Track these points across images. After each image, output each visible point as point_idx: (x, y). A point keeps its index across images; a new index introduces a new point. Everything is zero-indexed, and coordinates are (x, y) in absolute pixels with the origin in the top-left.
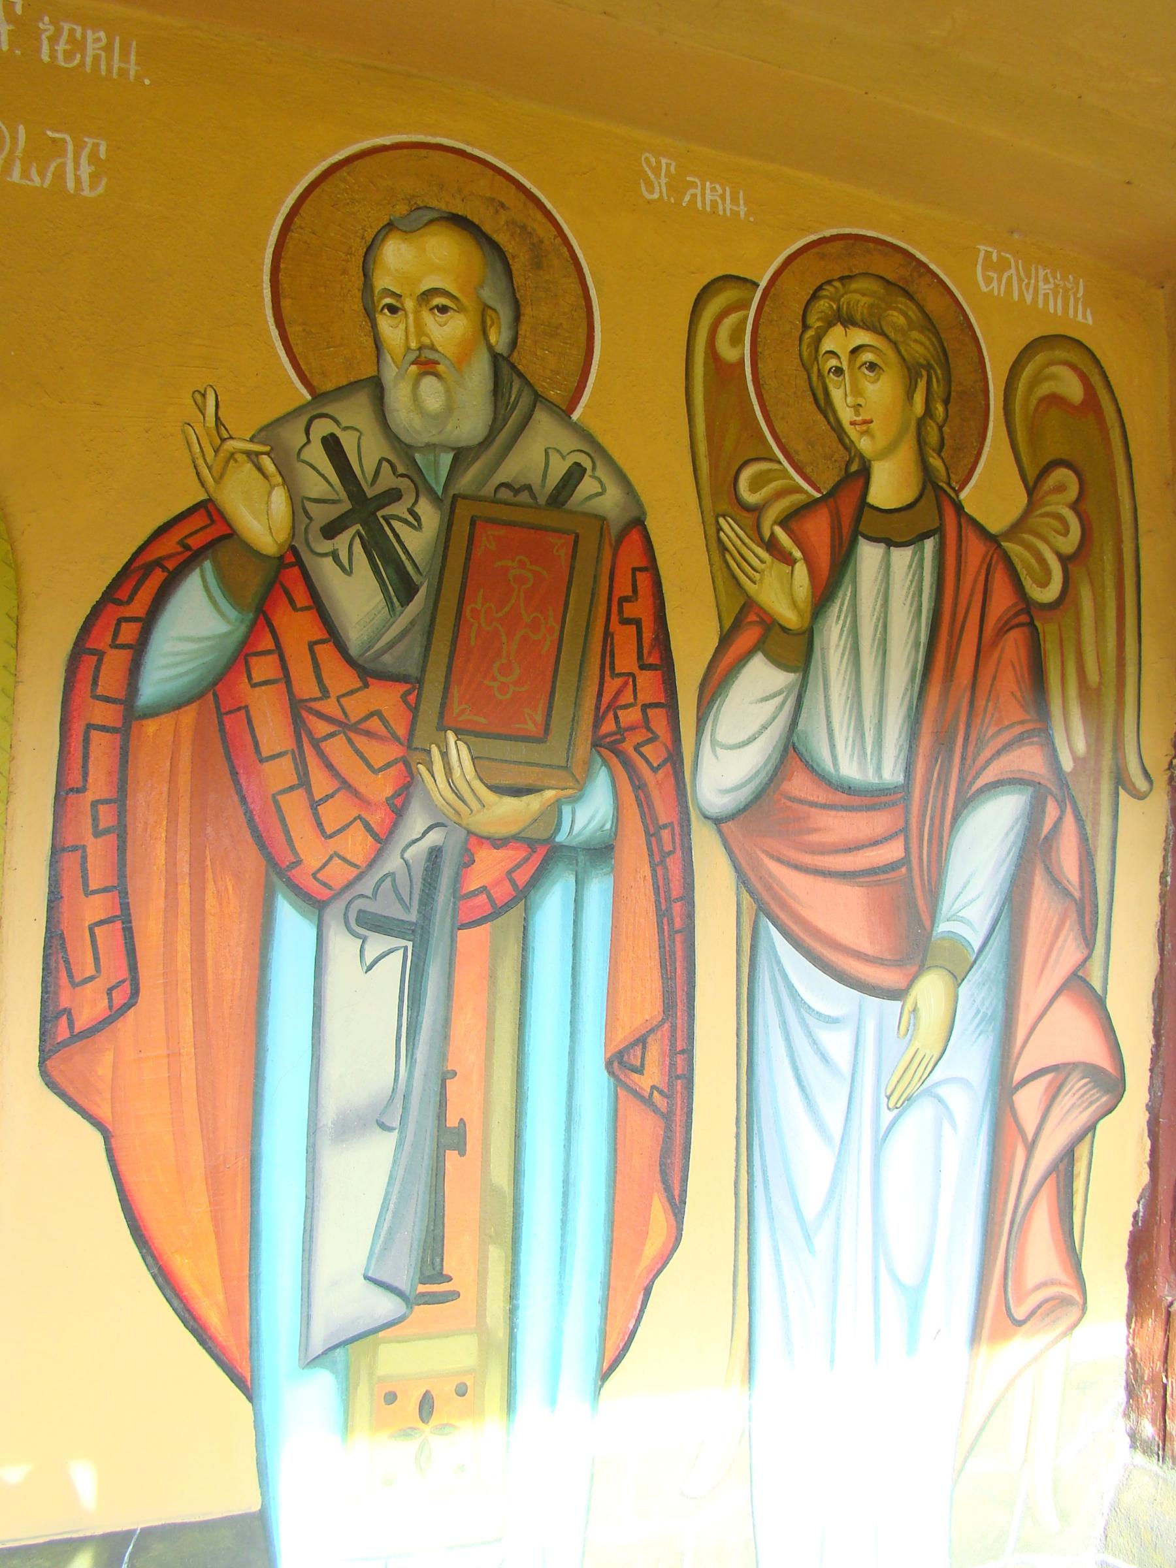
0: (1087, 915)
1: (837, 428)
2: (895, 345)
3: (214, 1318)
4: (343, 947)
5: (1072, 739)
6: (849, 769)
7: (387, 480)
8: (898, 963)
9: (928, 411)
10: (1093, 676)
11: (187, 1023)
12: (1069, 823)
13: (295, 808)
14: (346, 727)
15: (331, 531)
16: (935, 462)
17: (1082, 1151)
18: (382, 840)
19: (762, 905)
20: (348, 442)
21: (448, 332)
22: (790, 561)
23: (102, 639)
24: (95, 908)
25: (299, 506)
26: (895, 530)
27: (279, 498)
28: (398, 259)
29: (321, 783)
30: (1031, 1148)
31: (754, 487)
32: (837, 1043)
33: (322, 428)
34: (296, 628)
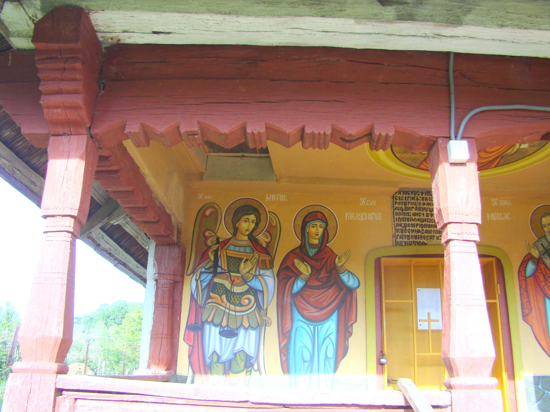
11: (538, 313)
15: (544, 254)
20: (543, 243)
25: (539, 252)
27: (537, 252)
28: (544, 220)
33: (540, 242)
34: (542, 266)
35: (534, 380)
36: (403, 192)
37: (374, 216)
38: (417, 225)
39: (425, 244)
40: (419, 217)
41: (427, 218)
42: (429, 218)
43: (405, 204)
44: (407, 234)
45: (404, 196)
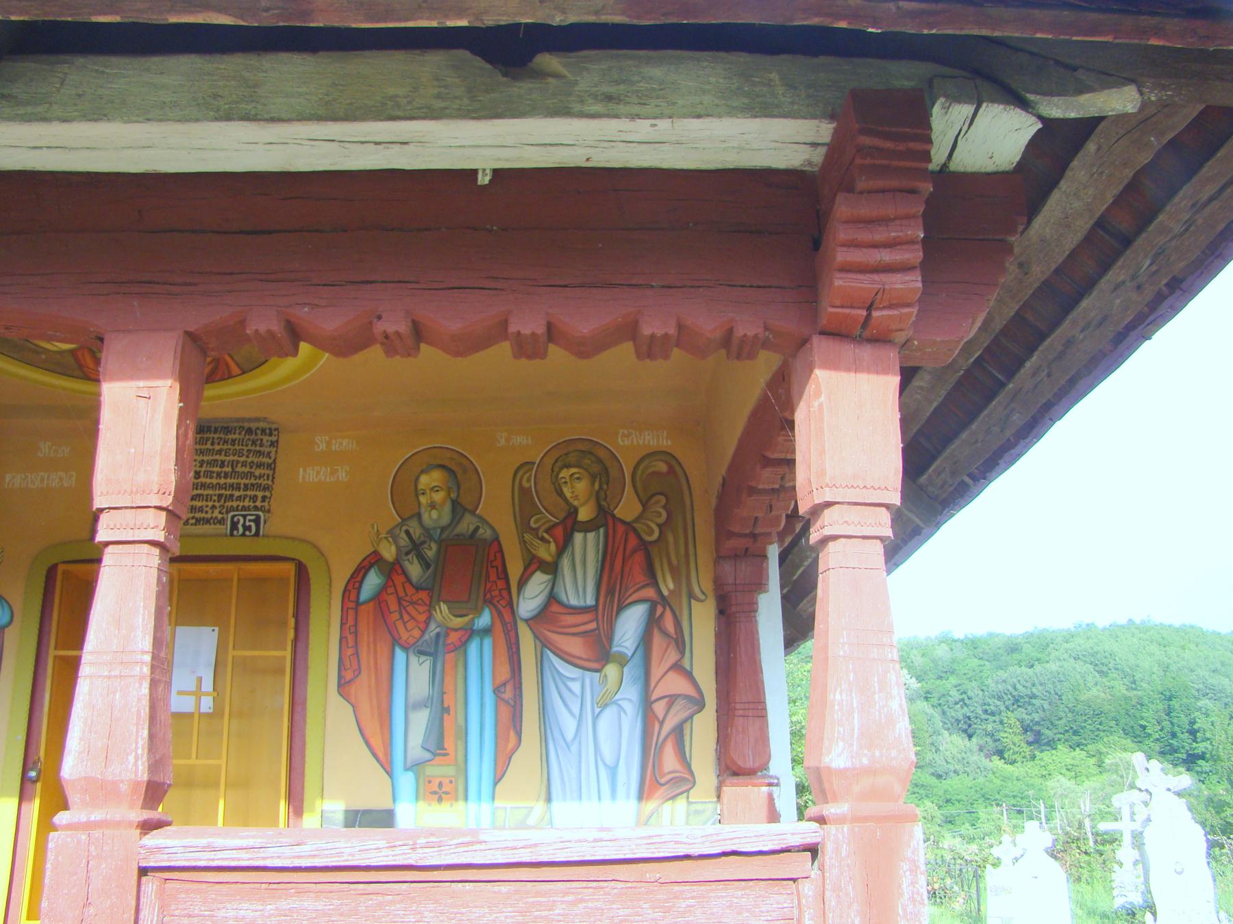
0: (680, 642)
1: (565, 499)
2: (586, 470)
3: (381, 755)
4: (414, 659)
5: (668, 585)
6: (573, 601)
7: (422, 539)
8: (597, 661)
9: (601, 487)
10: (674, 561)
11: (373, 680)
12: (668, 613)
13: (400, 625)
14: (412, 603)
15: (407, 554)
16: (603, 503)
17: (687, 726)
18: (423, 632)
19: (544, 644)
20: (411, 531)
21: (438, 497)
22: (549, 542)
23: (350, 587)
24: (350, 652)
25: (398, 549)
26: (587, 527)
27: (393, 548)
28: (424, 479)
29: (406, 617)
30: (662, 723)
31: (536, 522)
32: (576, 687)
33: (404, 528)
34: (399, 580)
35: (346, 818)
37: (61, 479)
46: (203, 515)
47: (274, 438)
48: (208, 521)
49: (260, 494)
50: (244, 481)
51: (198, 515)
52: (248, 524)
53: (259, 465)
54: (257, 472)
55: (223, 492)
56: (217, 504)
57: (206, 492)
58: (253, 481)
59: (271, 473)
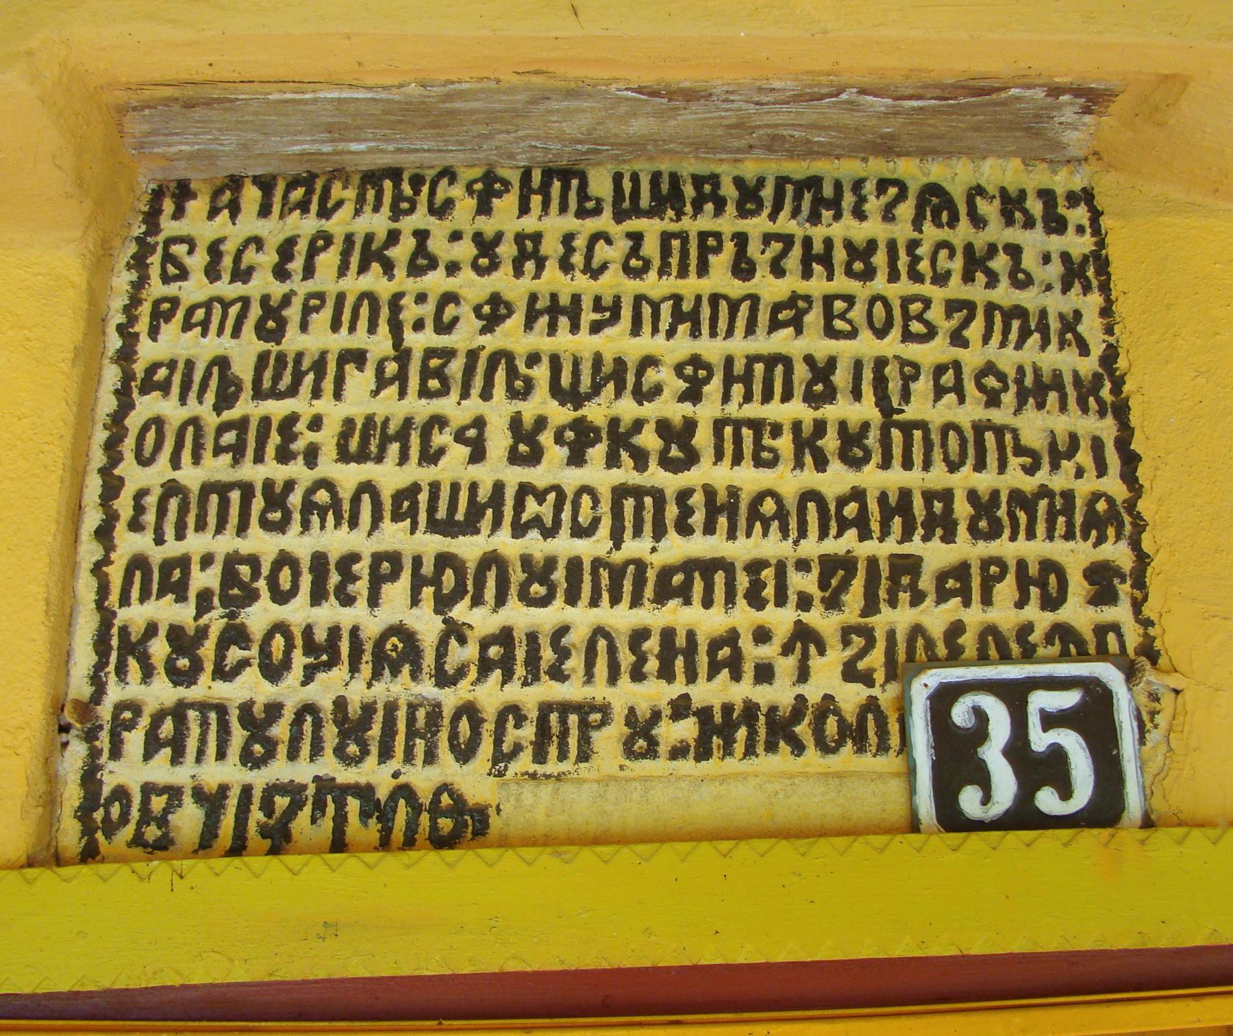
36: (266, 185)
38: (387, 566)
39: (462, 826)
40: (414, 473)
41: (514, 476)
42: (538, 476)
43: (272, 323)
44: (251, 687)
45: (273, 230)
46: (743, 691)
47: (1079, 245)
48: (780, 730)
49: (1075, 555)
50: (965, 479)
51: (713, 692)
52: (1040, 740)
53: (1038, 390)
54: (1035, 426)
55: (848, 542)
56: (816, 618)
57: (742, 549)
58: (1016, 478)
59: (1107, 428)
